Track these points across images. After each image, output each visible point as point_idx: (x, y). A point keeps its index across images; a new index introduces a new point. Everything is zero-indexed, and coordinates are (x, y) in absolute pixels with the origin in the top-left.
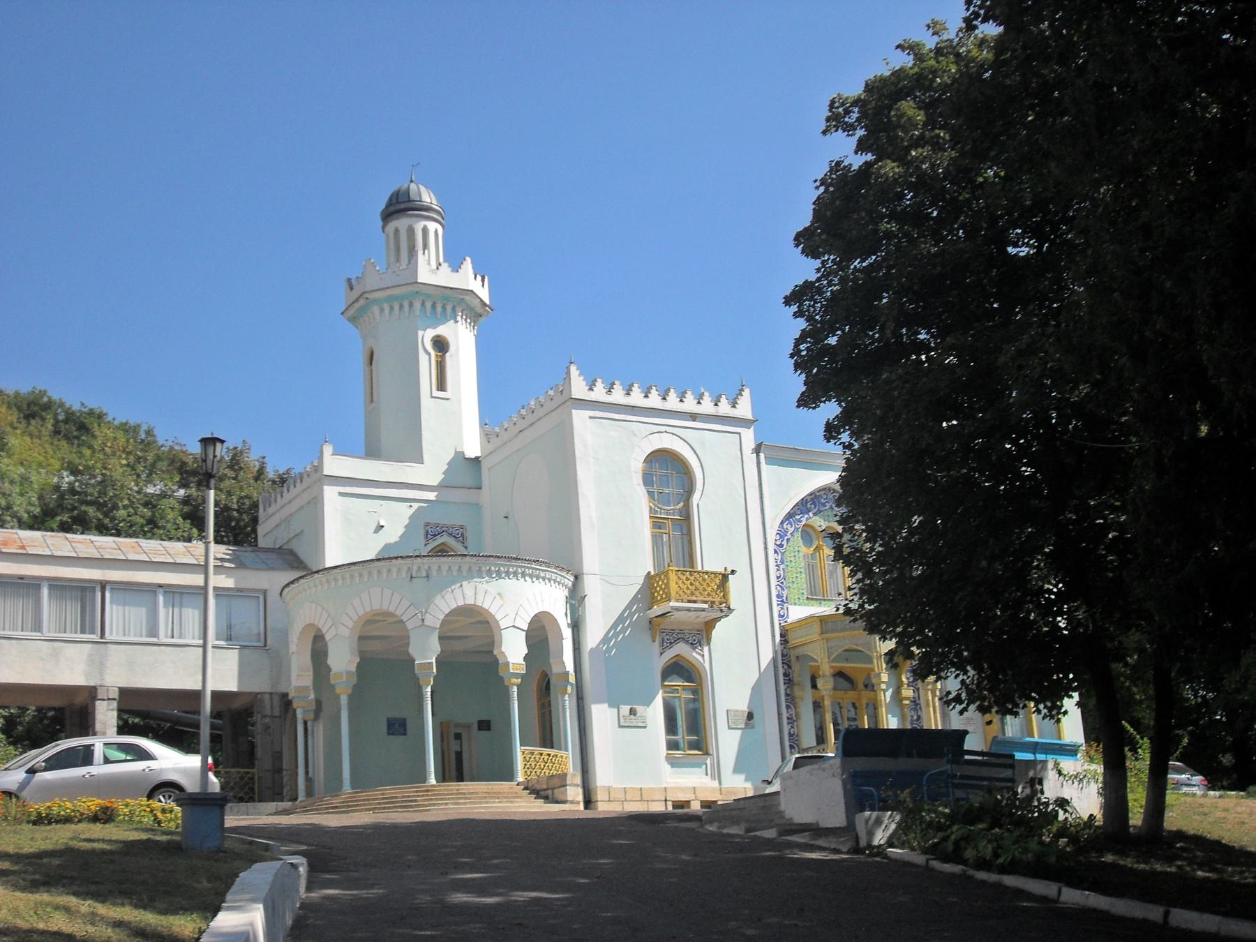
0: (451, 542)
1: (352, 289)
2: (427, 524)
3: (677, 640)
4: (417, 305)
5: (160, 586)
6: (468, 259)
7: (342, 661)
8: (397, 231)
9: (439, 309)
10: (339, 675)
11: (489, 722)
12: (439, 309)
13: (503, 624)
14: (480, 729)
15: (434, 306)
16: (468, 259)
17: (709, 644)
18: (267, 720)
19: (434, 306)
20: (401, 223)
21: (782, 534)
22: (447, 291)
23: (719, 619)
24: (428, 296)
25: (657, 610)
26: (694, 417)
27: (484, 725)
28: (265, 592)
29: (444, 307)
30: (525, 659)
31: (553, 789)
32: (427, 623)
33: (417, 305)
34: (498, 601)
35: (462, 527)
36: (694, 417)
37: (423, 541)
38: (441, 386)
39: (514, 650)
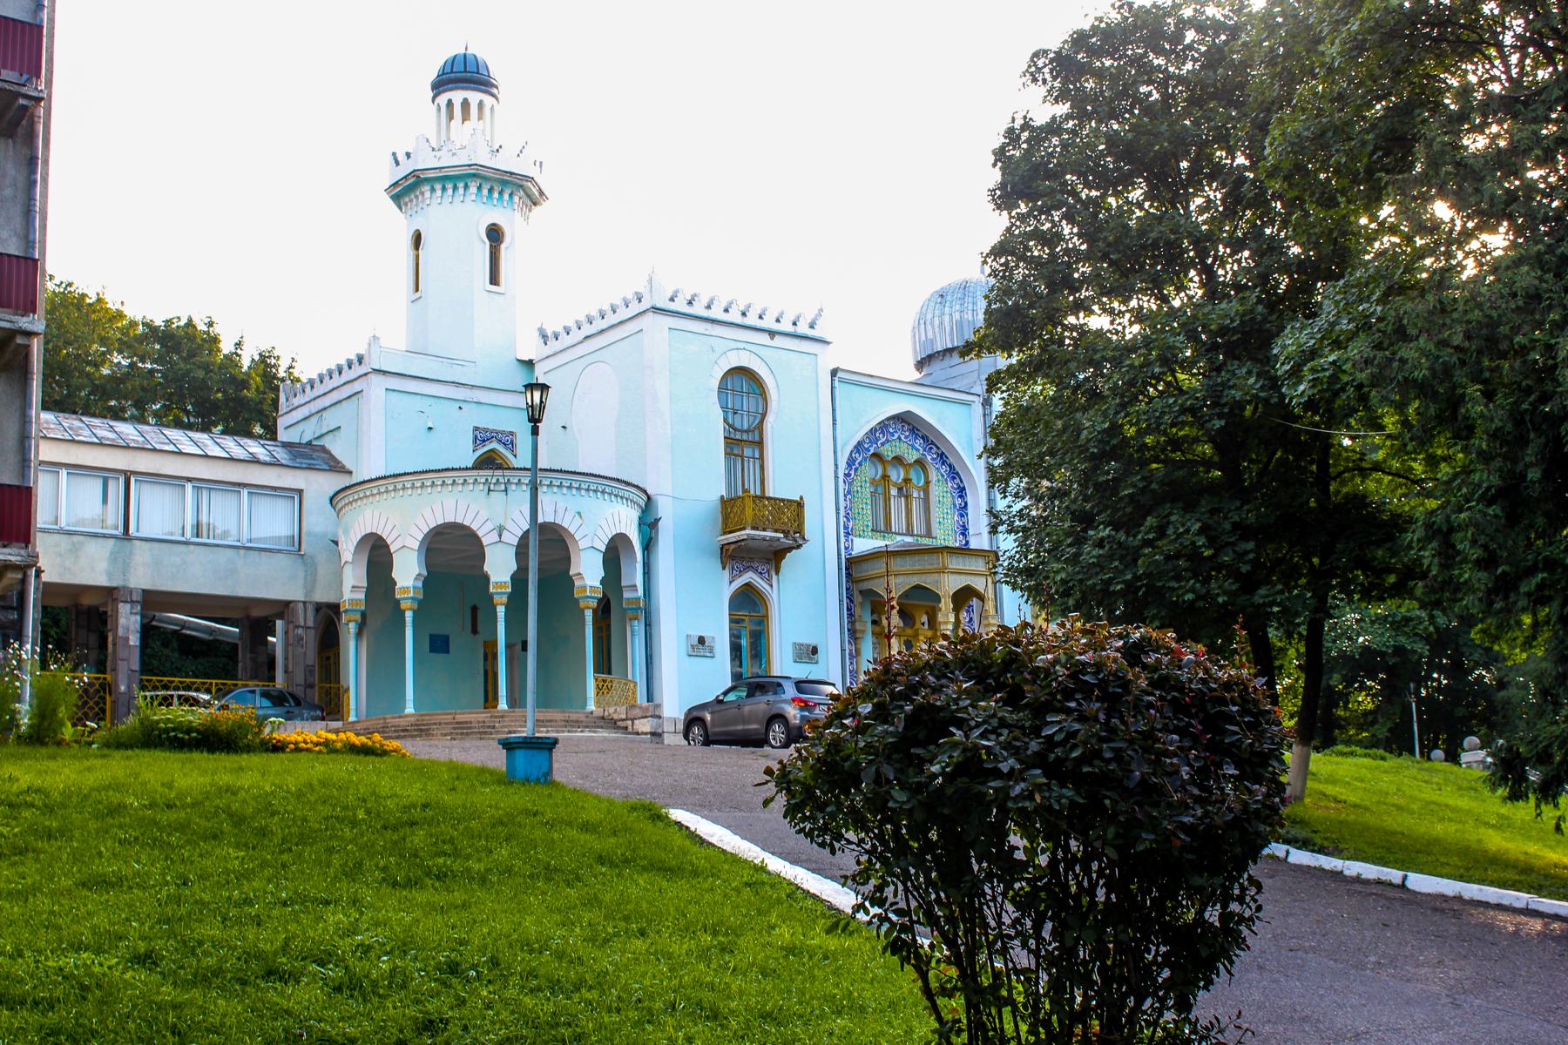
0: (501, 448)
1: (397, 163)
2: (476, 429)
3: (747, 569)
4: (473, 189)
5: (189, 480)
7: (407, 573)
8: (450, 103)
9: (496, 195)
10: (405, 590)
13: (582, 545)
17: (777, 573)
18: (300, 631)
19: (491, 190)
20: (457, 96)
21: (851, 462)
23: (790, 549)
24: (486, 179)
25: (732, 537)
26: (772, 334)
28: (300, 492)
29: (501, 193)
31: (633, 720)
34: (578, 521)
35: (512, 434)
36: (772, 334)
37: (471, 447)
38: (494, 279)
39: (589, 572)
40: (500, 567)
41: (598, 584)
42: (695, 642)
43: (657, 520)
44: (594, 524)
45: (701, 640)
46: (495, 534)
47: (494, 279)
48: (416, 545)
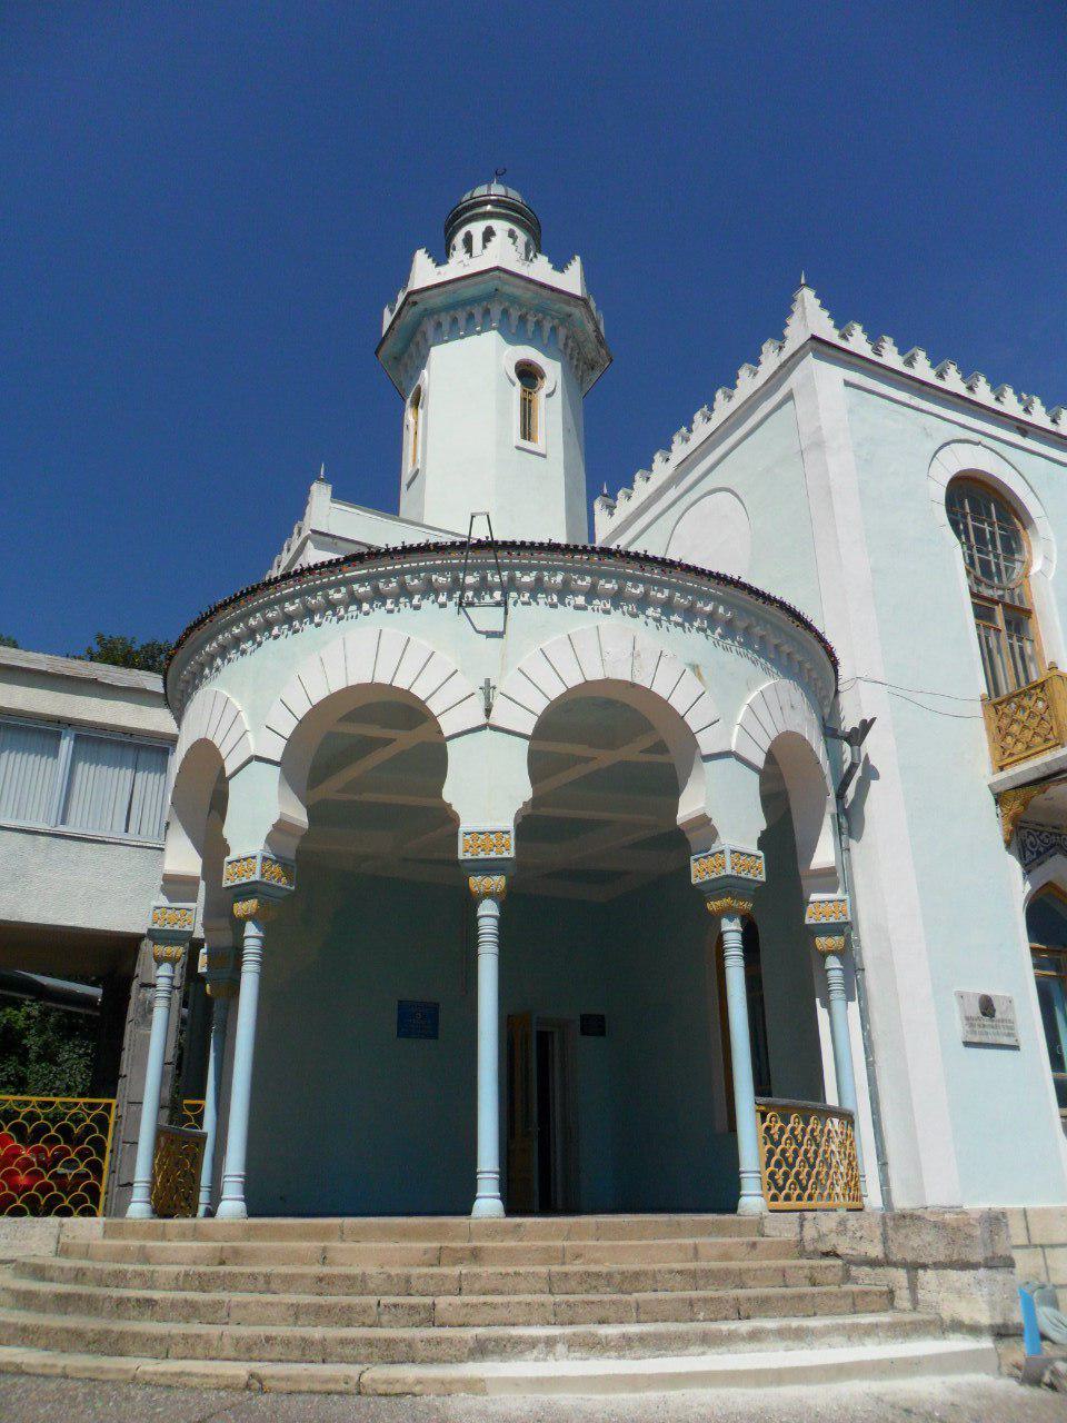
4: (496, 310)
6: (578, 258)
9: (531, 327)
11: (601, 1018)
12: (531, 327)
14: (584, 1032)
15: (523, 319)
16: (578, 258)
19: (523, 319)
22: (545, 293)
24: (514, 300)
26: (1024, 429)
27: (593, 1025)
29: (538, 324)
30: (762, 843)
32: (497, 718)
33: (496, 310)
36: (1024, 429)
40: (487, 794)
41: (753, 849)
42: (975, 1011)
43: (866, 726)
44: (729, 709)
45: (987, 1006)
46: (478, 703)
47: (527, 432)
48: (276, 750)
